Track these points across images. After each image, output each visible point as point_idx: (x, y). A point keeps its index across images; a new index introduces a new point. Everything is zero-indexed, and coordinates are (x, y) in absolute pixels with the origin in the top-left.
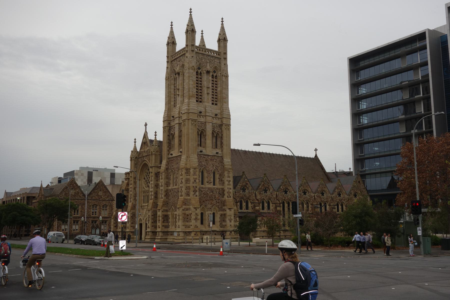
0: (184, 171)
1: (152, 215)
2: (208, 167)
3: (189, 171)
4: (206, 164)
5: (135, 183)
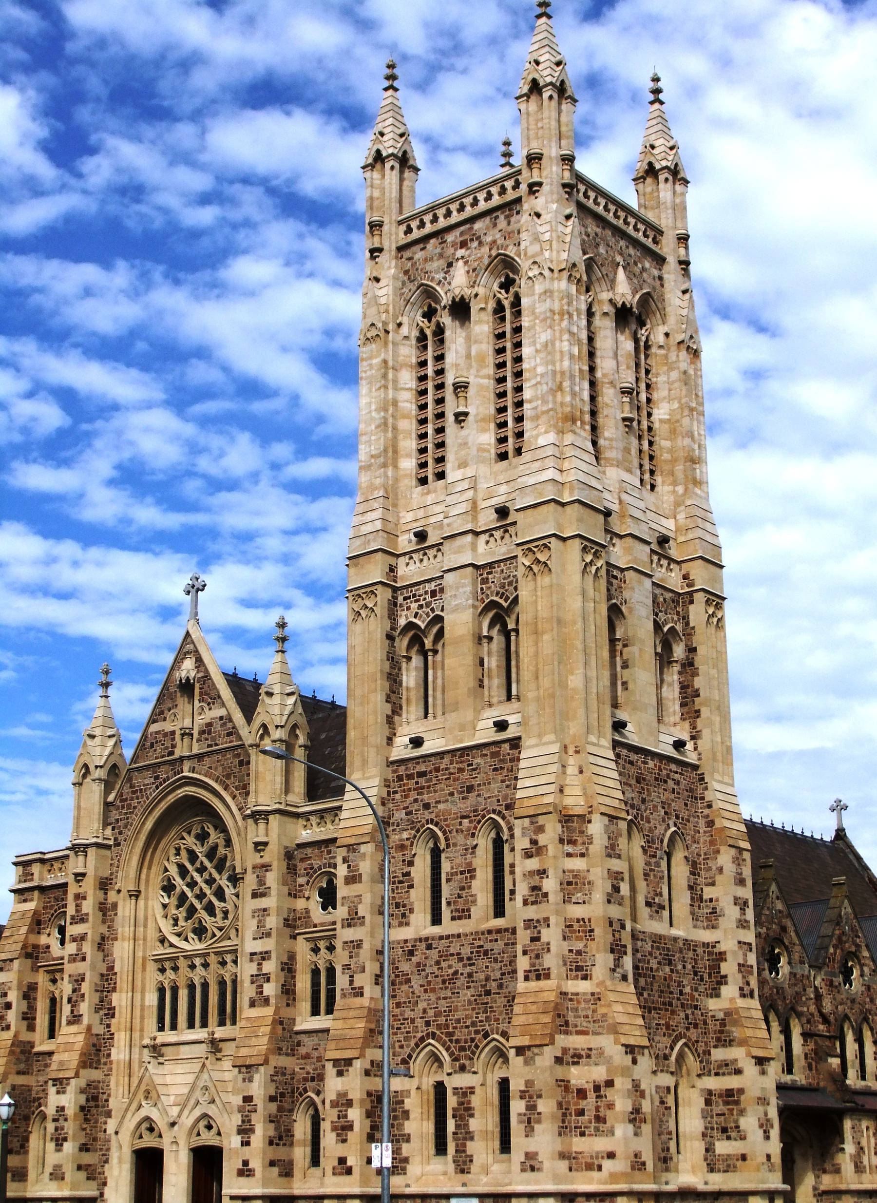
0: (552, 830)
1: (272, 1099)
3: (582, 832)
5: (106, 910)
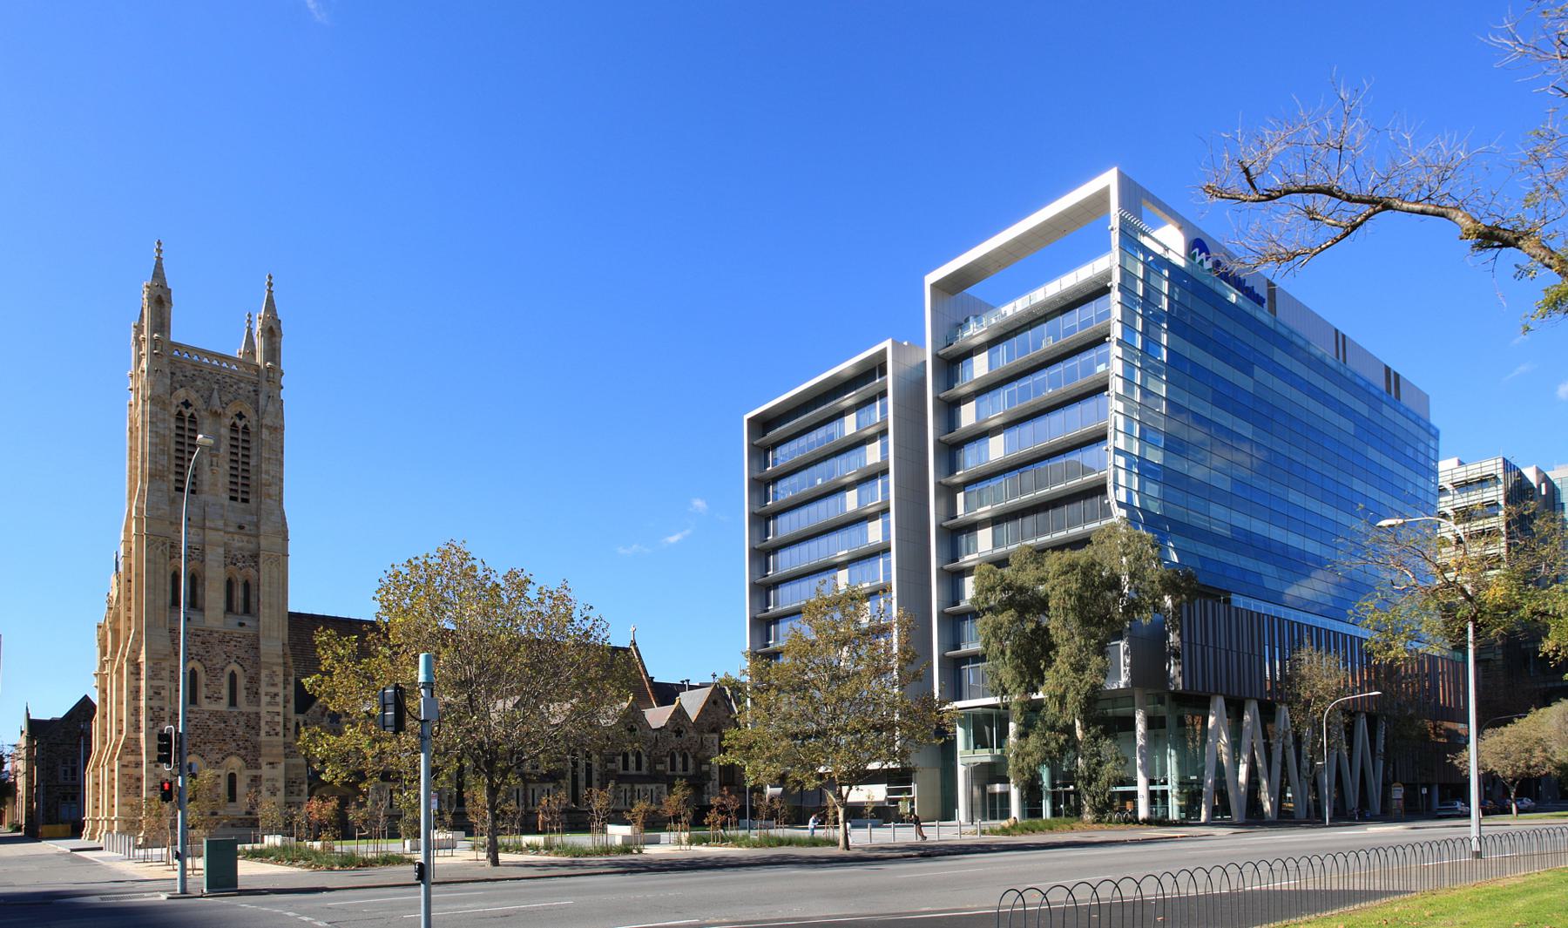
2: (211, 660)
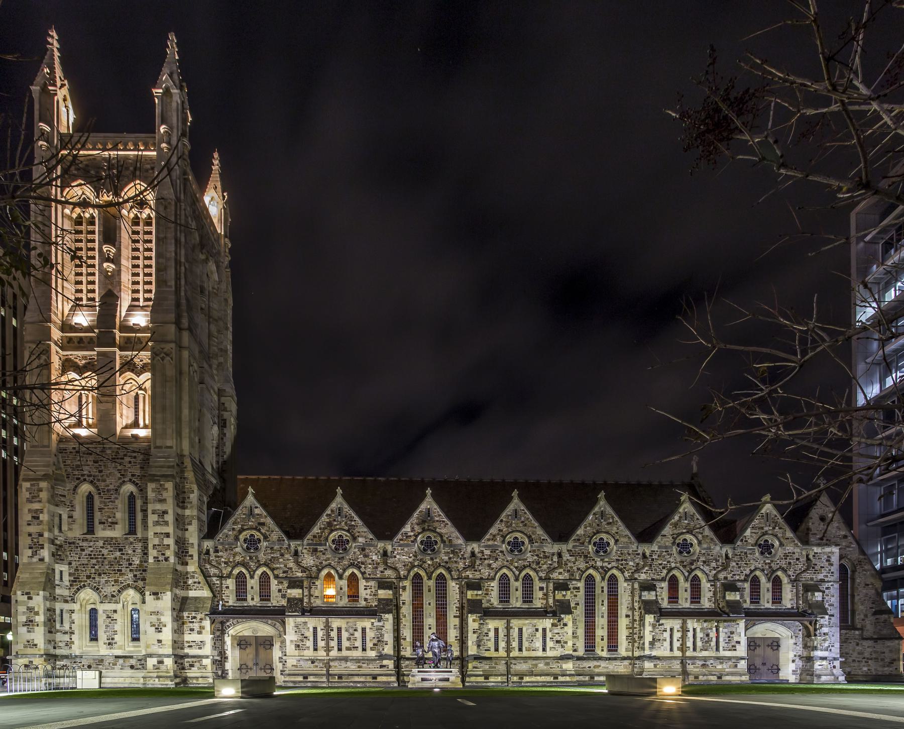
2: (104, 481)
4: (95, 472)
